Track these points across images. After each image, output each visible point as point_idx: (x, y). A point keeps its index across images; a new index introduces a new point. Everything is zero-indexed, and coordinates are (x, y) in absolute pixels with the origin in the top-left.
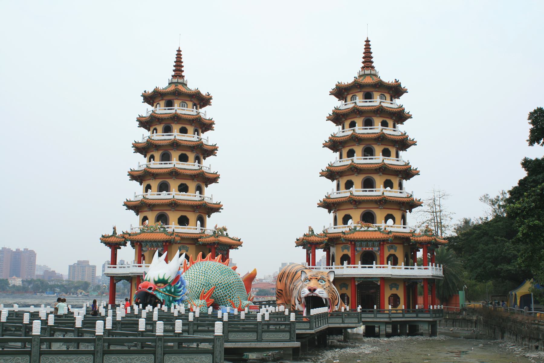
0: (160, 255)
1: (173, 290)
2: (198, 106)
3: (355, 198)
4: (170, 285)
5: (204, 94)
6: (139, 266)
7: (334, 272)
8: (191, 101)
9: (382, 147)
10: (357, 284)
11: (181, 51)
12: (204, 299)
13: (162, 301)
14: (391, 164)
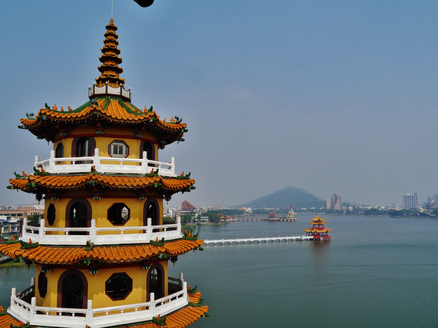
5: (168, 121)
11: (115, 29)
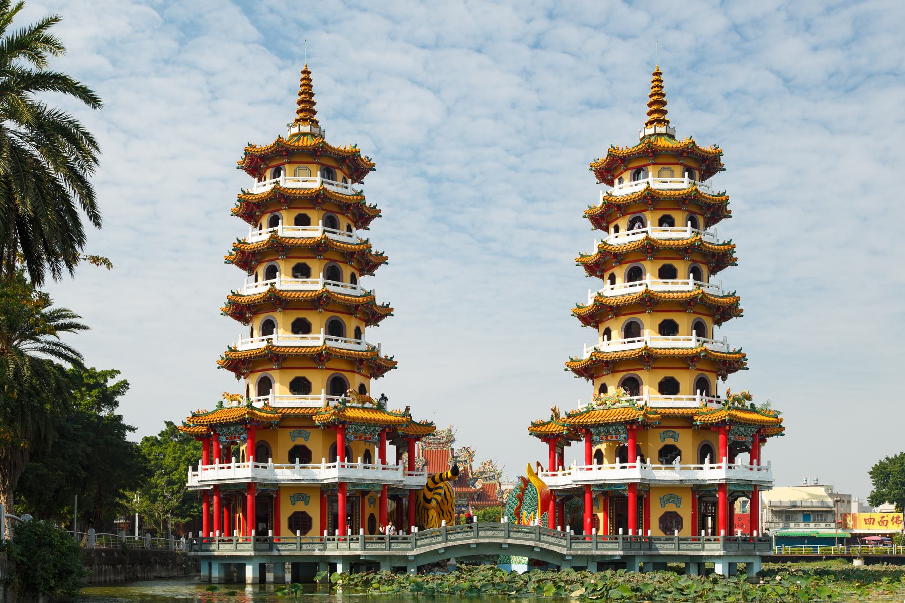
2: (697, 174)
6: (588, 469)
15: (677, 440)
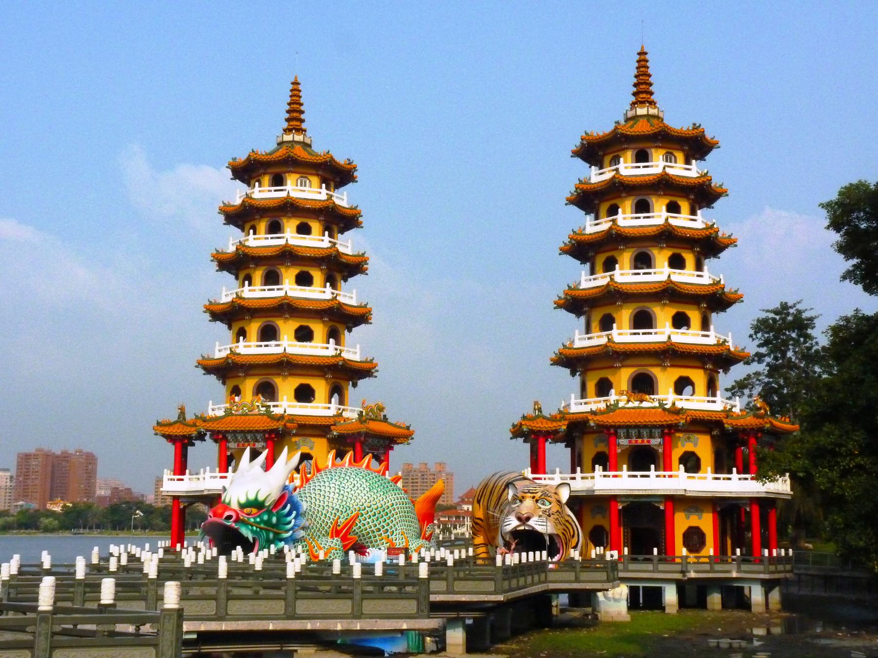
0: (254, 455)
1: (274, 520)
2: (332, 184)
3: (617, 346)
4: (269, 512)
5: (342, 162)
6: (221, 477)
7: (569, 485)
8: (318, 175)
9: (668, 253)
10: (620, 507)
11: (299, 84)
12: (337, 536)
13: (251, 540)
14: (686, 283)
15: (311, 448)
